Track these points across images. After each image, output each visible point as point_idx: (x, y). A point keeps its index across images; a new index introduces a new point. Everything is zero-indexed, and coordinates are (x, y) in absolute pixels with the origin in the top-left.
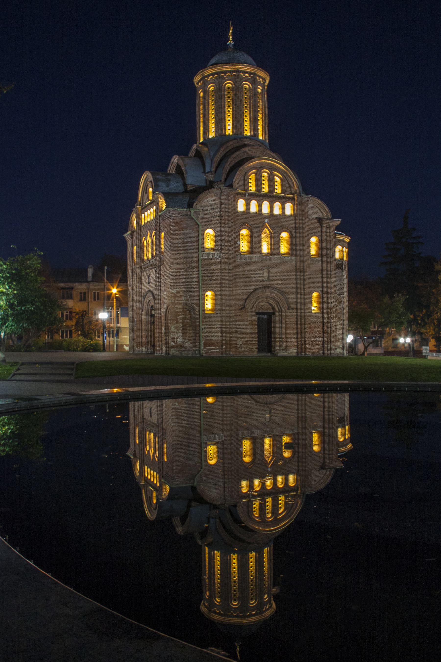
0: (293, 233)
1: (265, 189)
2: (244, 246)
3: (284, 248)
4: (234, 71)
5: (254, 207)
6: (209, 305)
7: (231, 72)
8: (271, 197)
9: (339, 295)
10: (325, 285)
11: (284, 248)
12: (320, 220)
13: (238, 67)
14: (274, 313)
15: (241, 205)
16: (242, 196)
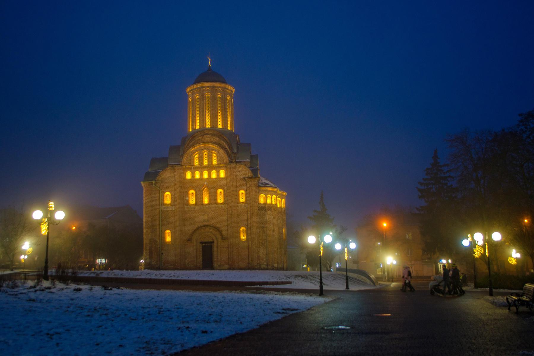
0: (226, 189)
1: (205, 163)
2: (192, 201)
3: (220, 200)
4: (200, 88)
5: (197, 176)
6: (168, 239)
7: (198, 88)
8: (210, 168)
9: (263, 227)
10: (249, 222)
11: (220, 200)
12: (244, 178)
13: (201, 84)
14: (213, 242)
15: (189, 175)
16: (189, 169)
